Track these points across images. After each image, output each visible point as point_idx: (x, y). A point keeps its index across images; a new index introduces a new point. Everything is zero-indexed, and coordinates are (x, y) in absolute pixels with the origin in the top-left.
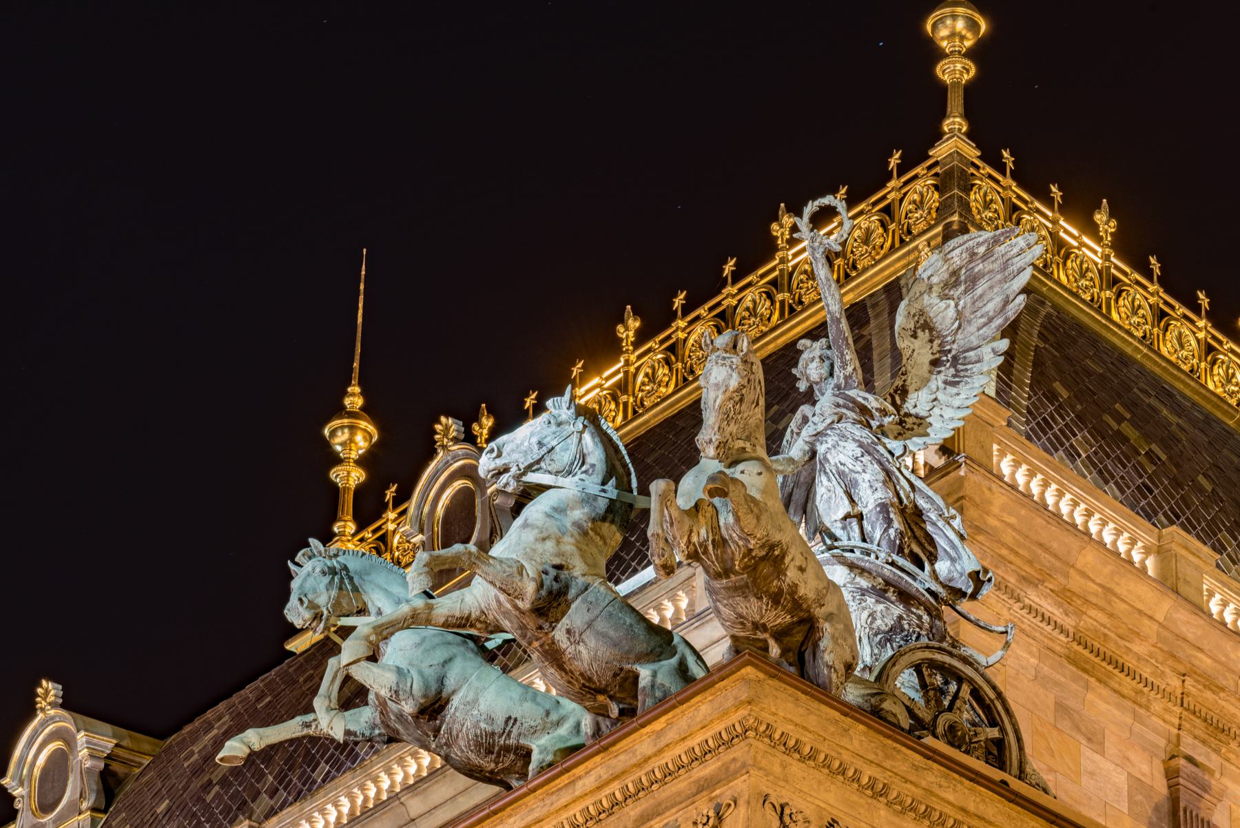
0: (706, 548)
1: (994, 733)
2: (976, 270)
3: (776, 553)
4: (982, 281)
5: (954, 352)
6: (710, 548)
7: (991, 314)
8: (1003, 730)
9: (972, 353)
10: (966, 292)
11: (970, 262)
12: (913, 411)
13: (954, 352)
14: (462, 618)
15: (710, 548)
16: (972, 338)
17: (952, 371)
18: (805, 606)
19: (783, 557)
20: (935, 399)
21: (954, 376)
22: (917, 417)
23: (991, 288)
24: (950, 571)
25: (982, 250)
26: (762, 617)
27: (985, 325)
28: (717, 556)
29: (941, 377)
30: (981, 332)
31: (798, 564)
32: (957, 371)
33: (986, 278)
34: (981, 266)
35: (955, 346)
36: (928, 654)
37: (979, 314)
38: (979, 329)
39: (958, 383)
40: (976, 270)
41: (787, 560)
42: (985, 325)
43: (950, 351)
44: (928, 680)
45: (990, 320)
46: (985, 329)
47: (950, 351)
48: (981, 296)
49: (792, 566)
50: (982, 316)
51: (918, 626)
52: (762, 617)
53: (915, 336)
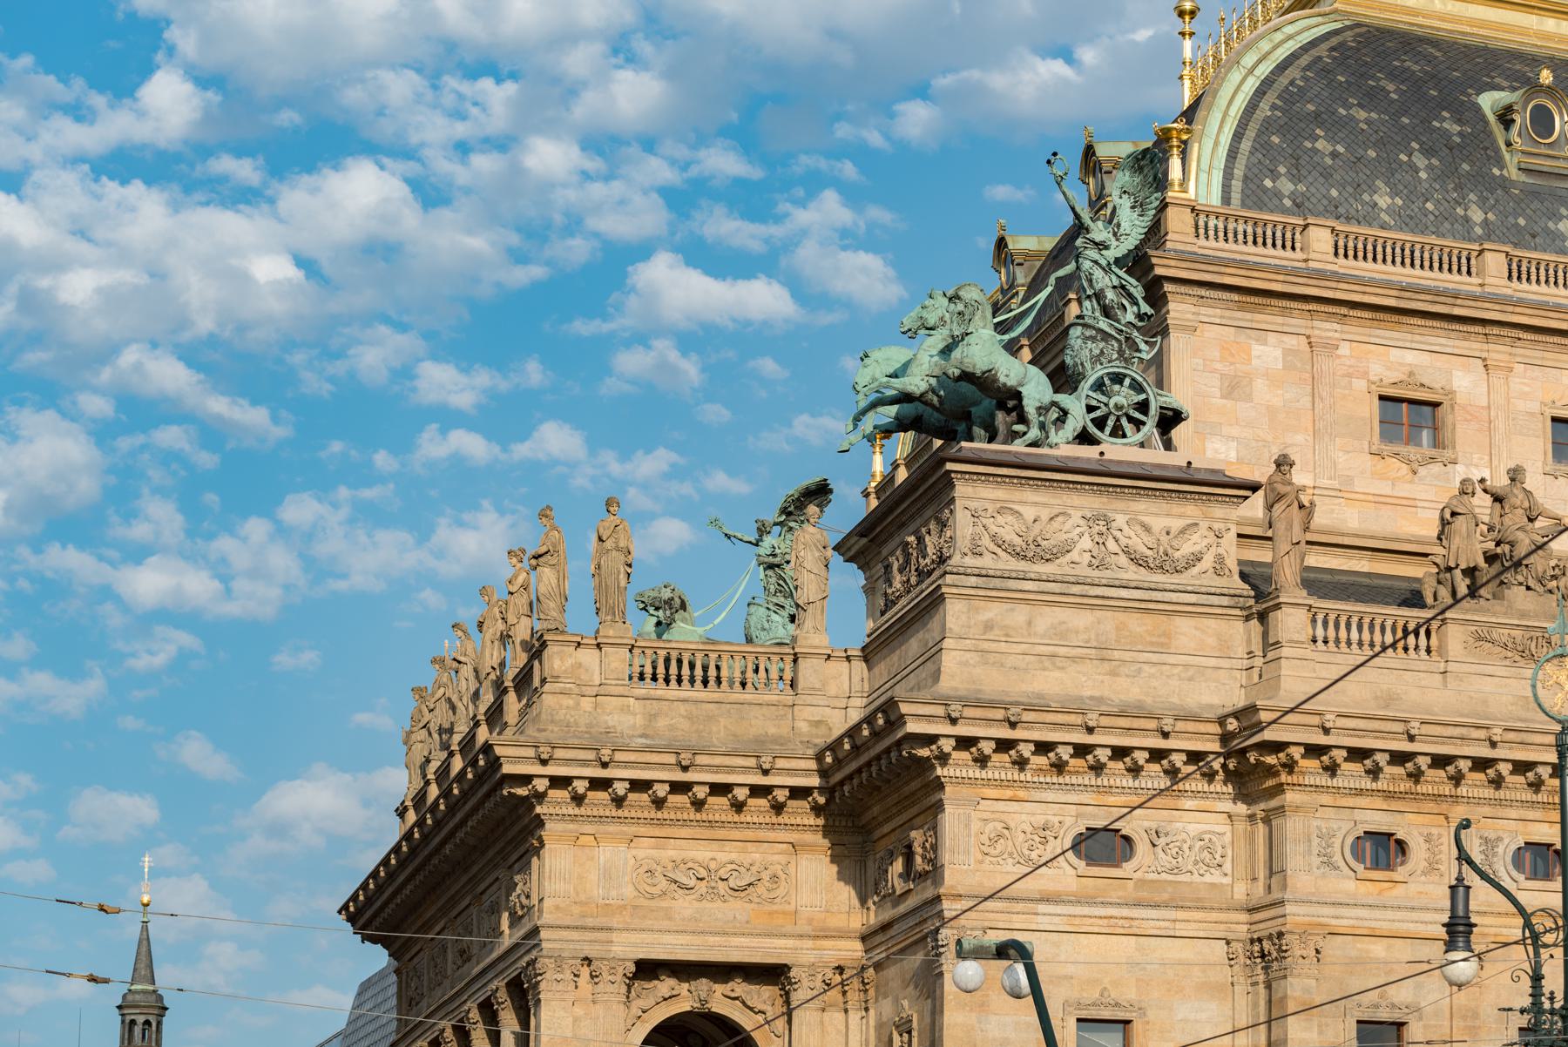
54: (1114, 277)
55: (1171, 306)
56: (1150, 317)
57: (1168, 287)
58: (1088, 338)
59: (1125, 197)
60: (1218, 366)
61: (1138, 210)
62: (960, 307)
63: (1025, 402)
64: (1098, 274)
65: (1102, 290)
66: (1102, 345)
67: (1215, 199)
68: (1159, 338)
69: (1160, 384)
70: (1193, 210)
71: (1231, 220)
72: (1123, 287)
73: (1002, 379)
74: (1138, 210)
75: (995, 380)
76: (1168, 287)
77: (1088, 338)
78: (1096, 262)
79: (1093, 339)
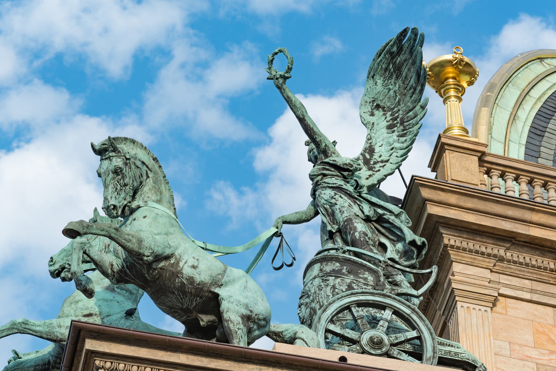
0: (125, 272)
1: (414, 334)
2: (398, 62)
3: (172, 262)
4: (404, 67)
5: (400, 116)
6: (128, 271)
7: (414, 85)
8: (419, 331)
9: (411, 113)
10: (397, 78)
11: (392, 58)
12: (380, 160)
13: (400, 116)
14: (45, 364)
15: (128, 271)
16: (409, 104)
17: (402, 128)
18: (206, 289)
19: (178, 263)
20: (392, 149)
21: (403, 130)
22: (382, 162)
23: (409, 70)
24: (404, 247)
25: (395, 49)
26: (182, 304)
27: (413, 93)
28: (133, 275)
29: (396, 133)
30: (413, 98)
31: (190, 264)
32: (404, 127)
33: (405, 65)
34: (399, 59)
35: (401, 112)
36: (354, 298)
37: (408, 88)
38: (411, 97)
39: (406, 134)
40: (398, 62)
41: (181, 264)
42: (413, 93)
43: (398, 117)
44: (356, 315)
45: (415, 89)
46: (414, 96)
47: (398, 117)
48: (406, 77)
49: (186, 267)
50: (410, 89)
51: (367, 285)
52: (182, 304)
53: (372, 114)
54: (366, 208)
55: (456, 267)
56: (420, 248)
57: (449, 239)
58: (329, 274)
59: (379, 113)
60: (534, 353)
61: (399, 129)
62: (118, 162)
63: (224, 305)
64: (343, 202)
65: (349, 221)
66: (349, 279)
67: (517, 152)
68: (435, 269)
69: (443, 331)
70: (481, 161)
71: (538, 182)
72: (380, 220)
73: (187, 271)
74: (399, 129)
75: (177, 274)
76: (449, 239)
77: (329, 274)
78: (339, 189)
79: (336, 274)
